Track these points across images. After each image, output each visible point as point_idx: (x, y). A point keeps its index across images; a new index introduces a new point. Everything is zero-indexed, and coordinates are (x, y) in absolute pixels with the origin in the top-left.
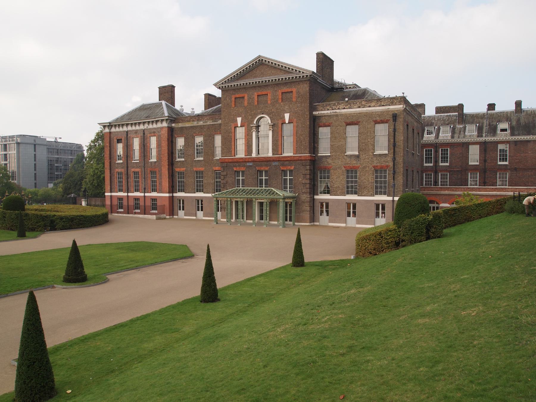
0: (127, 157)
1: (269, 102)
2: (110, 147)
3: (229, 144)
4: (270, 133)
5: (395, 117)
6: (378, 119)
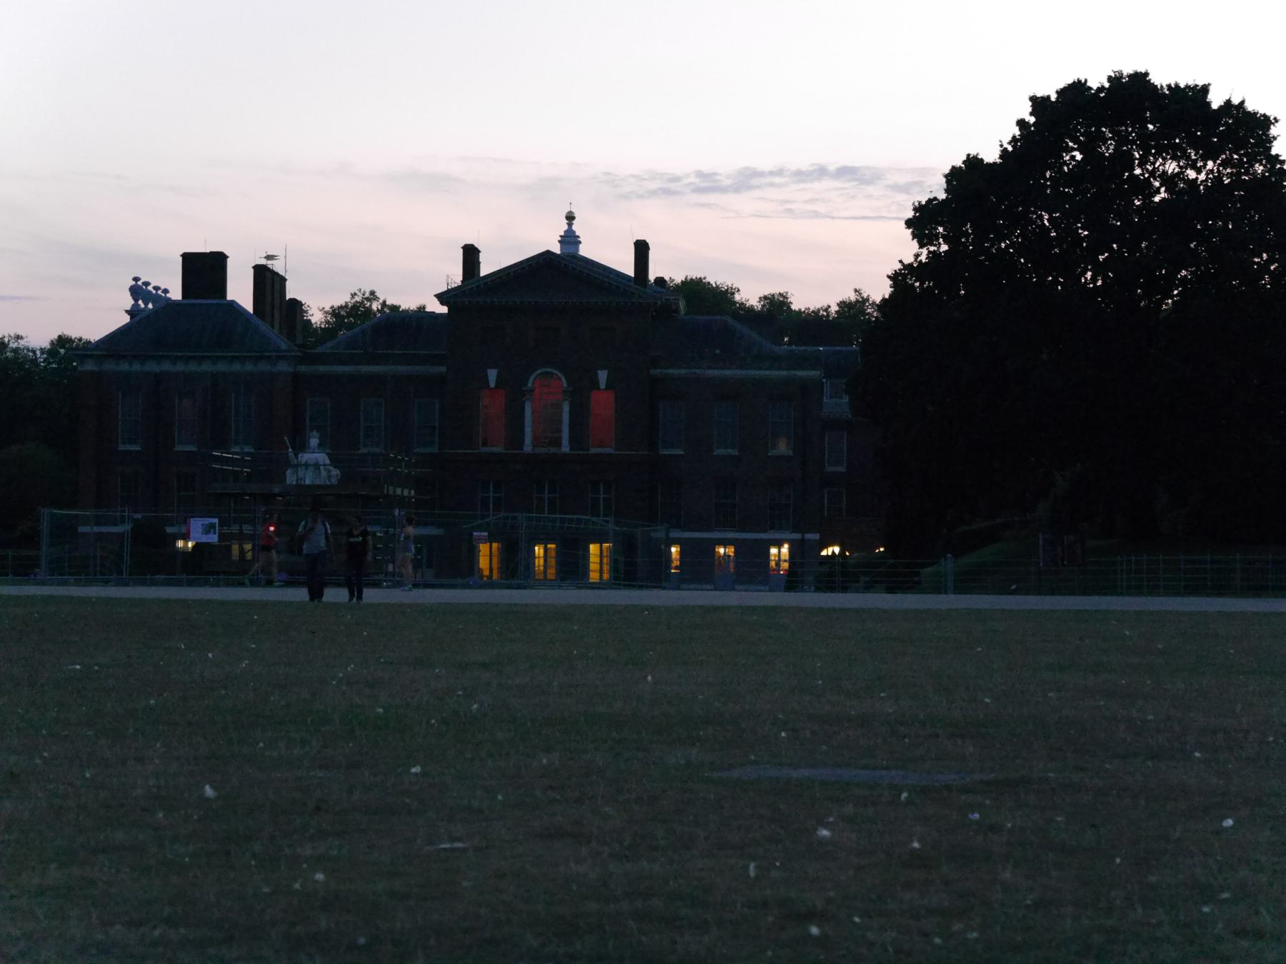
4: (566, 408)
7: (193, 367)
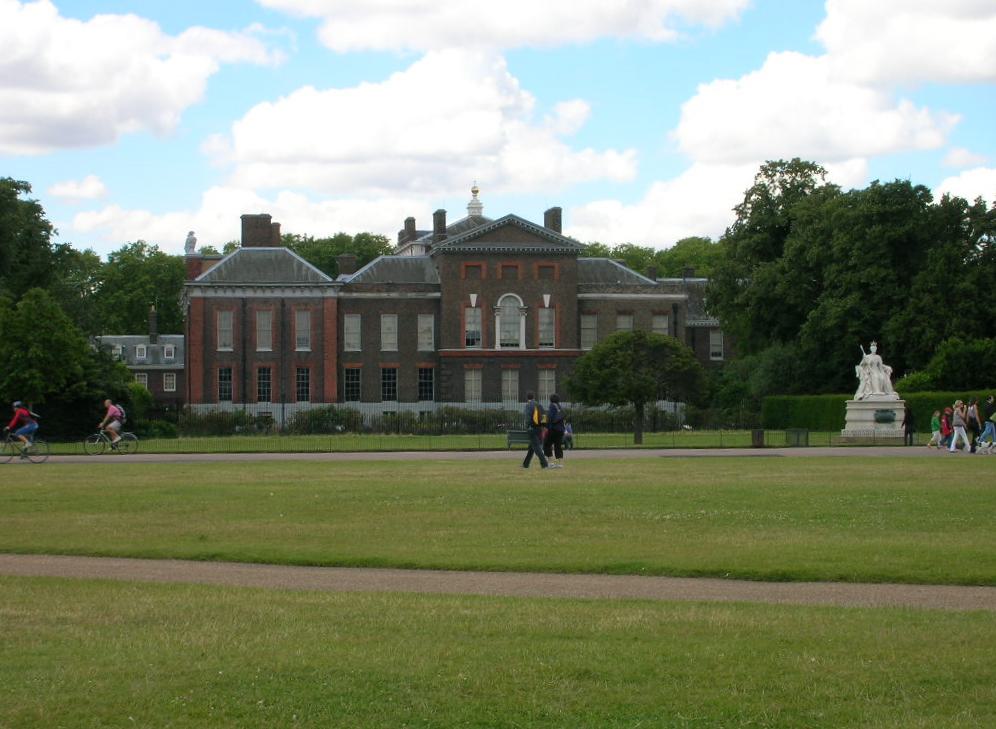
1: (520, 277)
2: (204, 322)
3: (449, 327)
4: (523, 321)
5: (676, 307)
6: (656, 309)
7: (268, 294)
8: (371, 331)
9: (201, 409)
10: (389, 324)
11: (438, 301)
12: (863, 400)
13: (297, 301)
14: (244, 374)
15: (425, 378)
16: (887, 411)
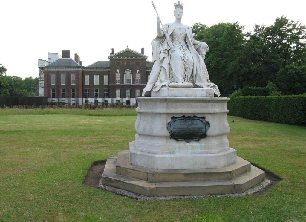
0: (58, 82)
2: (47, 77)
3: (112, 78)
7: (64, 70)
8: (92, 79)
9: (50, 100)
10: (96, 78)
11: (109, 71)
12: (153, 96)
13: (72, 72)
14: (58, 91)
15: (106, 92)
16: (193, 118)
